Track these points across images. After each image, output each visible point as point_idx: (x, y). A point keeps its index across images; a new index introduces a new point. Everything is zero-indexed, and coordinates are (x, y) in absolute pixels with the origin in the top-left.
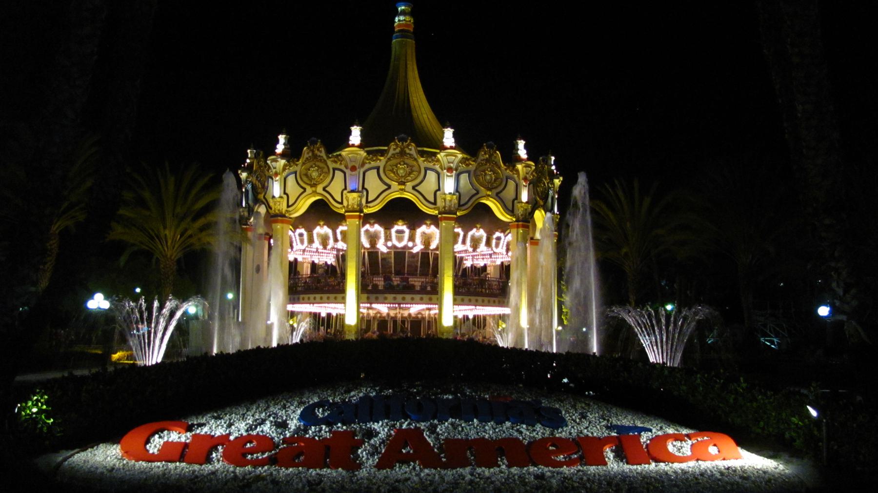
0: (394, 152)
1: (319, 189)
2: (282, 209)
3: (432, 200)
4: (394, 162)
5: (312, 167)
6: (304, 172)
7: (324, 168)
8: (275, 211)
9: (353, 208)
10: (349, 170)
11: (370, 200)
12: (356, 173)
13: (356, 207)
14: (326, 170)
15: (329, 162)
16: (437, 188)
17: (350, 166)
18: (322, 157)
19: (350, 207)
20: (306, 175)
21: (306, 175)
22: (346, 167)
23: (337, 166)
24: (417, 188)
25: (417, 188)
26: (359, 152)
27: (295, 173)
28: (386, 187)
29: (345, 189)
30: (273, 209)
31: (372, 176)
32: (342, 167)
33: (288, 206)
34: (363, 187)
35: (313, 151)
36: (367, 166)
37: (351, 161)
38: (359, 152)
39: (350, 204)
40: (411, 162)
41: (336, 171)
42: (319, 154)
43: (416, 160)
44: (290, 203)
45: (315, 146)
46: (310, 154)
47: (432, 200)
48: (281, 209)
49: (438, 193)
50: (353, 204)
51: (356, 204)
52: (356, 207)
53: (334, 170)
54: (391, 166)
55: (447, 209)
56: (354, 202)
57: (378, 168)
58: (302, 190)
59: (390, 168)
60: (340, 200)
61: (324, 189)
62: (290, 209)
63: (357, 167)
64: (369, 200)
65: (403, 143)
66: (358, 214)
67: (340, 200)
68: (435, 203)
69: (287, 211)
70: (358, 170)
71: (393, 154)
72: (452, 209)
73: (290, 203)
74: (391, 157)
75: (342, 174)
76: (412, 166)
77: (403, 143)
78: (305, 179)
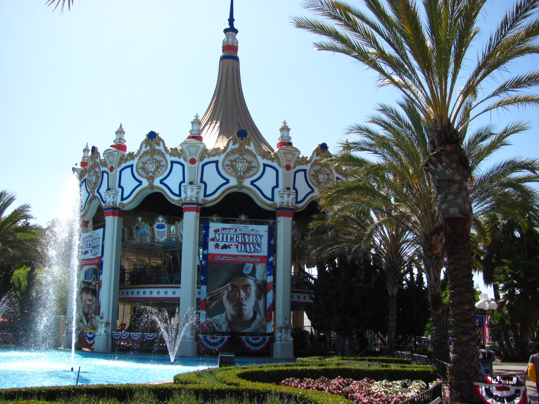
0: (233, 147)
1: (157, 182)
2: (116, 202)
3: (270, 197)
4: (233, 157)
5: (149, 160)
6: (141, 165)
7: (162, 161)
8: (109, 204)
9: (192, 200)
10: (188, 163)
11: (208, 193)
12: (196, 165)
13: (194, 199)
14: (163, 163)
15: (168, 156)
16: (275, 184)
17: (189, 159)
18: (160, 150)
19: (188, 199)
20: (143, 168)
21: (143, 168)
22: (185, 160)
23: (176, 159)
24: (255, 183)
26: (198, 145)
27: (132, 166)
28: (225, 181)
29: (184, 181)
30: (107, 202)
31: (210, 169)
32: (181, 160)
33: (123, 199)
34: (202, 181)
35: (151, 146)
36: (206, 160)
37: (191, 154)
38: (198, 145)
39: (188, 196)
40: (249, 158)
41: (174, 164)
42: (157, 147)
43: (255, 156)
44: (125, 196)
45: (153, 139)
46: (148, 148)
47: (270, 197)
48: (115, 202)
49: (276, 190)
50: (191, 196)
51: (194, 196)
52: (194, 199)
53: (172, 162)
54: (229, 160)
55: (285, 204)
56: (192, 194)
57: (217, 162)
58: (138, 183)
59: (229, 163)
60: (177, 193)
61: (161, 182)
62: (125, 202)
63: (197, 159)
64: (208, 193)
65: (242, 139)
66: (196, 206)
67: (177, 193)
68: (272, 199)
69: (120, 203)
70: (197, 163)
71: (232, 149)
72: (290, 205)
73: (125, 196)
74: (230, 152)
75: (181, 167)
76: (250, 163)
77: (242, 139)
78: (142, 173)
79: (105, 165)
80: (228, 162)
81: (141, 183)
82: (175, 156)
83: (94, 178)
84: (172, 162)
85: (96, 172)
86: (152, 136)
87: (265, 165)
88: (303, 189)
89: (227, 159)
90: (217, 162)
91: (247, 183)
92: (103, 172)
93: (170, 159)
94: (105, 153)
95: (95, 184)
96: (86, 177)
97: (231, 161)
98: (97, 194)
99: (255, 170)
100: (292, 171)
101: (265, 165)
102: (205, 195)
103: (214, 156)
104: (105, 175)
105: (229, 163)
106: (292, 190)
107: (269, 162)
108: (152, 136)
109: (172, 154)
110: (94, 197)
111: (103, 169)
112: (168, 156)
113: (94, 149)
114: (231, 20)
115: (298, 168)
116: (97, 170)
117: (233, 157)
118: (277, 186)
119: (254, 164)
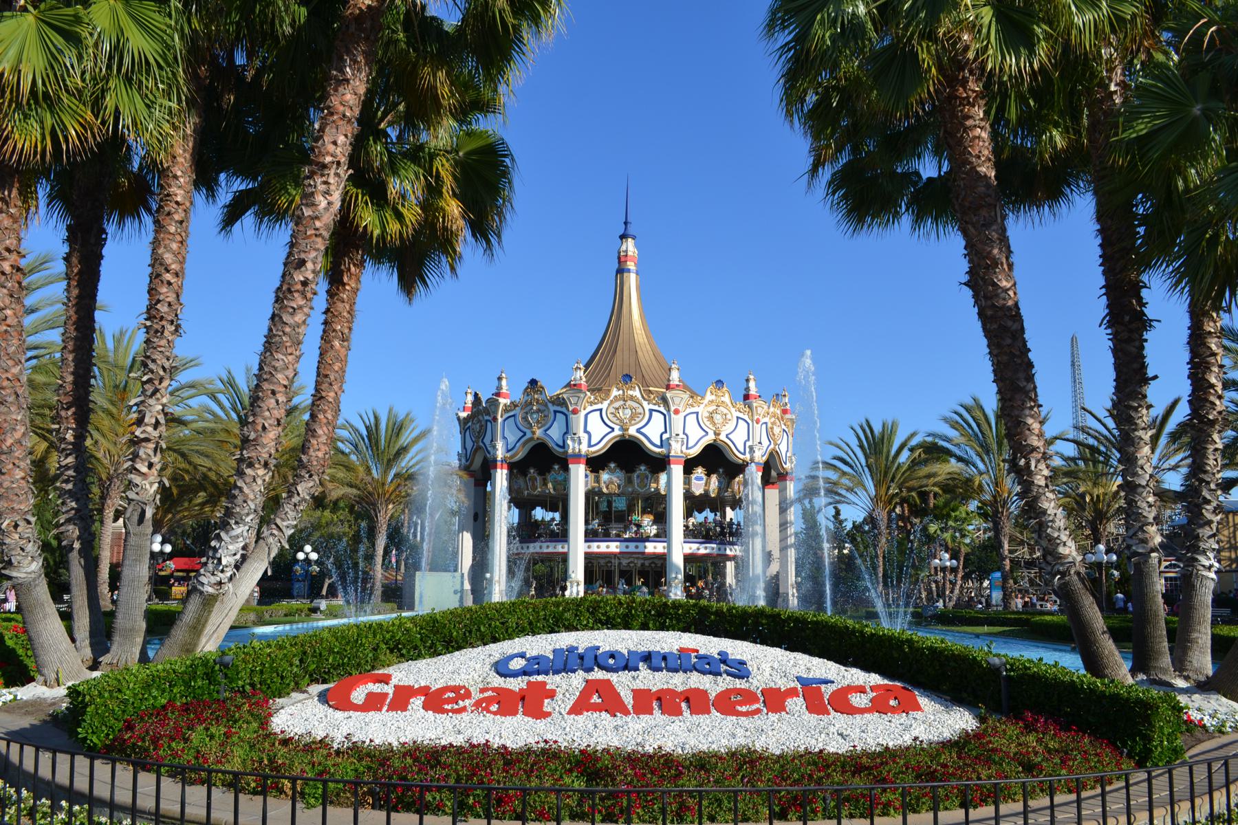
4: (617, 404)
11: (593, 443)
23: (559, 408)
25: (642, 430)
32: (564, 410)
57: (601, 410)
59: (613, 410)
64: (593, 443)
79: (488, 414)
80: (611, 410)
81: (525, 434)
82: (558, 405)
83: (478, 426)
84: (555, 412)
85: (479, 421)
86: (533, 382)
87: (651, 411)
88: (694, 433)
89: (611, 408)
90: (601, 410)
91: (632, 431)
92: (487, 421)
93: (552, 408)
94: (487, 401)
95: (479, 433)
96: (470, 424)
97: (617, 409)
98: (481, 444)
99: (641, 416)
100: (682, 415)
101: (651, 411)
102: (590, 446)
103: (595, 404)
104: (489, 424)
105: (613, 410)
106: (682, 435)
107: (656, 407)
108: (533, 382)
109: (553, 403)
110: (479, 448)
111: (487, 418)
112: (550, 405)
113: (476, 395)
114: (626, 223)
115: (688, 411)
116: (480, 417)
117: (617, 404)
118: (666, 432)
119: (640, 410)
